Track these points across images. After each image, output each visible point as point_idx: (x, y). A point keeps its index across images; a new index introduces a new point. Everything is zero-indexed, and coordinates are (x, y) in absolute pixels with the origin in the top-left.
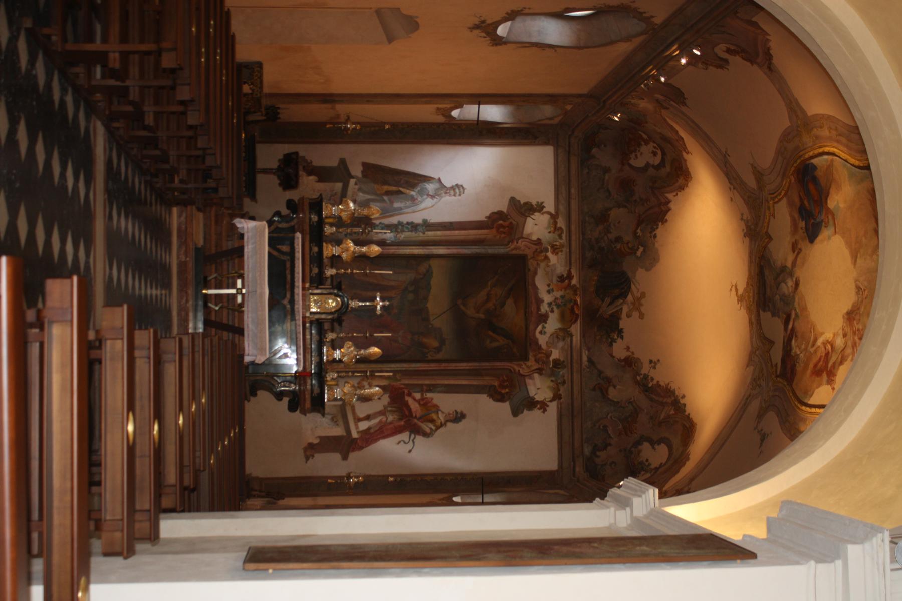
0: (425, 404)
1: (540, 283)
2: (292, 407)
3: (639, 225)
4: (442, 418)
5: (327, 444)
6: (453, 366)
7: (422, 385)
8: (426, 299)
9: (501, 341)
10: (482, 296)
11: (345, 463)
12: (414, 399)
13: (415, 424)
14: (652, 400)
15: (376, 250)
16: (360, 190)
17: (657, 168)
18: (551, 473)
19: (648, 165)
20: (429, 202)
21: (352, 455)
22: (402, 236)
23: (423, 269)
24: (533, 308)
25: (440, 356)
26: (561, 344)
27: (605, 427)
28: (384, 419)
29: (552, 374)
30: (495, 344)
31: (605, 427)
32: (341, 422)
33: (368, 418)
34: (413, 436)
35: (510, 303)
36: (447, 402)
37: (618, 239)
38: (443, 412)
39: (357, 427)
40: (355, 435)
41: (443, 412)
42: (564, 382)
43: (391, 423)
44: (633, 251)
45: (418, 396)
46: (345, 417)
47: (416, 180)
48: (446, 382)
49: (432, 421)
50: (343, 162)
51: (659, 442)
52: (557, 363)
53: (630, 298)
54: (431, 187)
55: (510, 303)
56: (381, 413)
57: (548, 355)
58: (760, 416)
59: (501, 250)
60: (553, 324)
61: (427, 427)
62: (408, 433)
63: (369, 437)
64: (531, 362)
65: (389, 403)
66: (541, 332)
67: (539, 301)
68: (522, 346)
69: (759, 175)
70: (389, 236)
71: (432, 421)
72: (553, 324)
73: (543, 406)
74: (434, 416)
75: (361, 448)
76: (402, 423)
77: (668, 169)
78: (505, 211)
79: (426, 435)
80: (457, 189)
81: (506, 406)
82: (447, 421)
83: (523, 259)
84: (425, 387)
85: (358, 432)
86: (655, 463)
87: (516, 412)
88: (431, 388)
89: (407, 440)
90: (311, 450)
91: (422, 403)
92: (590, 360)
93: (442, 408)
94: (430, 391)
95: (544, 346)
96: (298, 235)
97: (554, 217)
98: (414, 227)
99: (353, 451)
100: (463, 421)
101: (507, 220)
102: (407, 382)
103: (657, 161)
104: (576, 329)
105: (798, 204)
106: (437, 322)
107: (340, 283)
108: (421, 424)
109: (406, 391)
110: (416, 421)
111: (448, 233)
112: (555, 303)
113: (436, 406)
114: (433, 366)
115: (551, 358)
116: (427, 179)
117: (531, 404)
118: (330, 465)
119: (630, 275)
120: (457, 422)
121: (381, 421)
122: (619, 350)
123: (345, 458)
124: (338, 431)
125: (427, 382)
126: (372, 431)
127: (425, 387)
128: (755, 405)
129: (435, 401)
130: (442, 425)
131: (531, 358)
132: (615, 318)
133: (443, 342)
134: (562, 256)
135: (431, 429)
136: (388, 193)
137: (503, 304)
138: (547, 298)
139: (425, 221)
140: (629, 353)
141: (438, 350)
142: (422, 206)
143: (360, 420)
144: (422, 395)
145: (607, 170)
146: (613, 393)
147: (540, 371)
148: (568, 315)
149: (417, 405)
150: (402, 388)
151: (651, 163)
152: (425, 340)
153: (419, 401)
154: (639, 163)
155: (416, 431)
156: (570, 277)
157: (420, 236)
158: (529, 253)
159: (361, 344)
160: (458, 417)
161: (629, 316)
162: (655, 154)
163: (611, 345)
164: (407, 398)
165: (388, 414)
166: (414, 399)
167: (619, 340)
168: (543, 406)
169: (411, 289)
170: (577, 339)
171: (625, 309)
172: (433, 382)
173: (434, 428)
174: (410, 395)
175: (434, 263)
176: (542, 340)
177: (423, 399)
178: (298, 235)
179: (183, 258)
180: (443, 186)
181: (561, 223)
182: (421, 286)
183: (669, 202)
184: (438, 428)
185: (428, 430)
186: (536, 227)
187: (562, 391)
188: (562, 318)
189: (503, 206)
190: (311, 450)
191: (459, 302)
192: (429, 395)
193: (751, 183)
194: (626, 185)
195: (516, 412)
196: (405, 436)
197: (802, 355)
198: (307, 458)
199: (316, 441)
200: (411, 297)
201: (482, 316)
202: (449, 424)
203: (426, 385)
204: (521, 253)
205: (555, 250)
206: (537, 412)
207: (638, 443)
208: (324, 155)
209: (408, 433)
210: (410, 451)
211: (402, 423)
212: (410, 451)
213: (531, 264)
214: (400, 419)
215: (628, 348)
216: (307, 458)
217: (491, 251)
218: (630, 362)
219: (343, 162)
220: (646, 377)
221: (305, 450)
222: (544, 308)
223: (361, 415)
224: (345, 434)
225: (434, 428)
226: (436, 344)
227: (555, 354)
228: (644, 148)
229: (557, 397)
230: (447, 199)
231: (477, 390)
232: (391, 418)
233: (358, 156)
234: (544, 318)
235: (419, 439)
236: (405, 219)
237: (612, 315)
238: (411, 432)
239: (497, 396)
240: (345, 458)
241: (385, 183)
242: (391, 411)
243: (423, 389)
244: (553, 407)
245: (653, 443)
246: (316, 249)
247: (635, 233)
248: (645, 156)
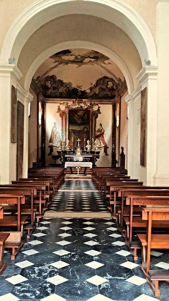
0: (98, 131)
1: (74, 107)
2: (99, 158)
3: (63, 86)
5: (105, 151)
6: (90, 126)
8: (77, 131)
9: (86, 116)
10: (76, 119)
14: (99, 85)
15: (68, 141)
16: (55, 143)
17: (51, 82)
18: (113, 106)
19: (50, 84)
20: (57, 130)
21: (108, 146)
22: (64, 135)
23: (71, 131)
24: (79, 109)
25: (89, 129)
26: (87, 103)
27: (104, 94)
29: (93, 105)
30: (86, 117)
31: (104, 94)
32: (101, 148)
33: (100, 143)
35: (78, 114)
36: (98, 127)
37: (66, 90)
42: (95, 103)
44: (68, 87)
45: (96, 133)
46: (100, 147)
47: (53, 132)
49: (102, 130)
50: (49, 147)
51: (108, 84)
52: (91, 104)
53: (78, 88)
54: (54, 129)
55: (78, 114)
56: (100, 140)
57: (89, 106)
58: (105, 64)
59: (67, 115)
60: (82, 105)
61: (103, 131)
63: (104, 143)
64: (90, 109)
66: (84, 107)
67: (78, 107)
68: (87, 111)
69: (56, 62)
70: (64, 138)
71: (102, 130)
72: (82, 105)
73: (99, 107)
75: (106, 144)
77: (51, 79)
78: (59, 114)
79: (104, 131)
80: (55, 123)
81: (99, 115)
83: (70, 111)
86: (112, 85)
87: (100, 113)
88: (95, 130)
90: (106, 154)
92: (90, 97)
95: (87, 107)
96: (65, 156)
97: (61, 104)
98: (62, 132)
101: (62, 114)
103: (49, 82)
104: (84, 100)
105: (63, 54)
106: (82, 129)
107: (74, 148)
111: (64, 126)
112: (79, 103)
114: (90, 129)
115: (90, 105)
116: (53, 129)
117: (99, 110)
118: (109, 151)
119: (73, 88)
122: (88, 91)
123: (108, 148)
124: (103, 149)
125: (94, 131)
128: (102, 64)
131: (89, 109)
132: (81, 91)
133: (86, 127)
134: (69, 102)
136: (55, 138)
137: (79, 115)
138: (77, 106)
139: (61, 130)
140: (89, 89)
141: (87, 128)
142: (58, 131)
145: (51, 92)
146: (97, 93)
147: (92, 108)
148: (81, 102)
151: (50, 83)
152: (85, 131)
154: (50, 86)
155: (103, 133)
156: (73, 101)
157: (64, 131)
158: (68, 110)
159: (87, 144)
160: (101, 125)
161: (81, 89)
162: (48, 82)
163: (87, 93)
167: (86, 91)
168: (99, 107)
169: (75, 134)
170: (86, 100)
171: (80, 90)
175: (70, 129)
176: (86, 107)
178: (65, 156)
179: (73, 178)
180: (54, 126)
181: (62, 102)
182: (74, 132)
183: (58, 80)
186: (63, 108)
187: (96, 103)
188: (81, 103)
189: (58, 114)
190: (106, 154)
191: (78, 124)
192: (96, 131)
193: (57, 63)
194: (54, 88)
195: (100, 113)
197: (94, 55)
198: (108, 155)
199: (105, 153)
200: (77, 134)
201: (81, 119)
204: (68, 111)
205: (67, 104)
206: (100, 109)
207: (107, 87)
208: (48, 150)
213: (70, 109)
215: (88, 89)
216: (108, 155)
217: (68, 117)
218: (91, 89)
219: (49, 147)
220: (94, 86)
221: (106, 155)
222: (79, 106)
226: (86, 129)
227: (89, 104)
228: (47, 85)
229: (97, 104)
230: (57, 126)
231: (95, 121)
233: (48, 144)
234: (81, 107)
236: (61, 135)
237: (81, 92)
238: (103, 134)
239: (97, 117)
240: (108, 148)
241: (53, 138)
243: (95, 132)
244: (99, 105)
245: (108, 85)
246: (68, 153)
247: (65, 87)
248: (49, 84)
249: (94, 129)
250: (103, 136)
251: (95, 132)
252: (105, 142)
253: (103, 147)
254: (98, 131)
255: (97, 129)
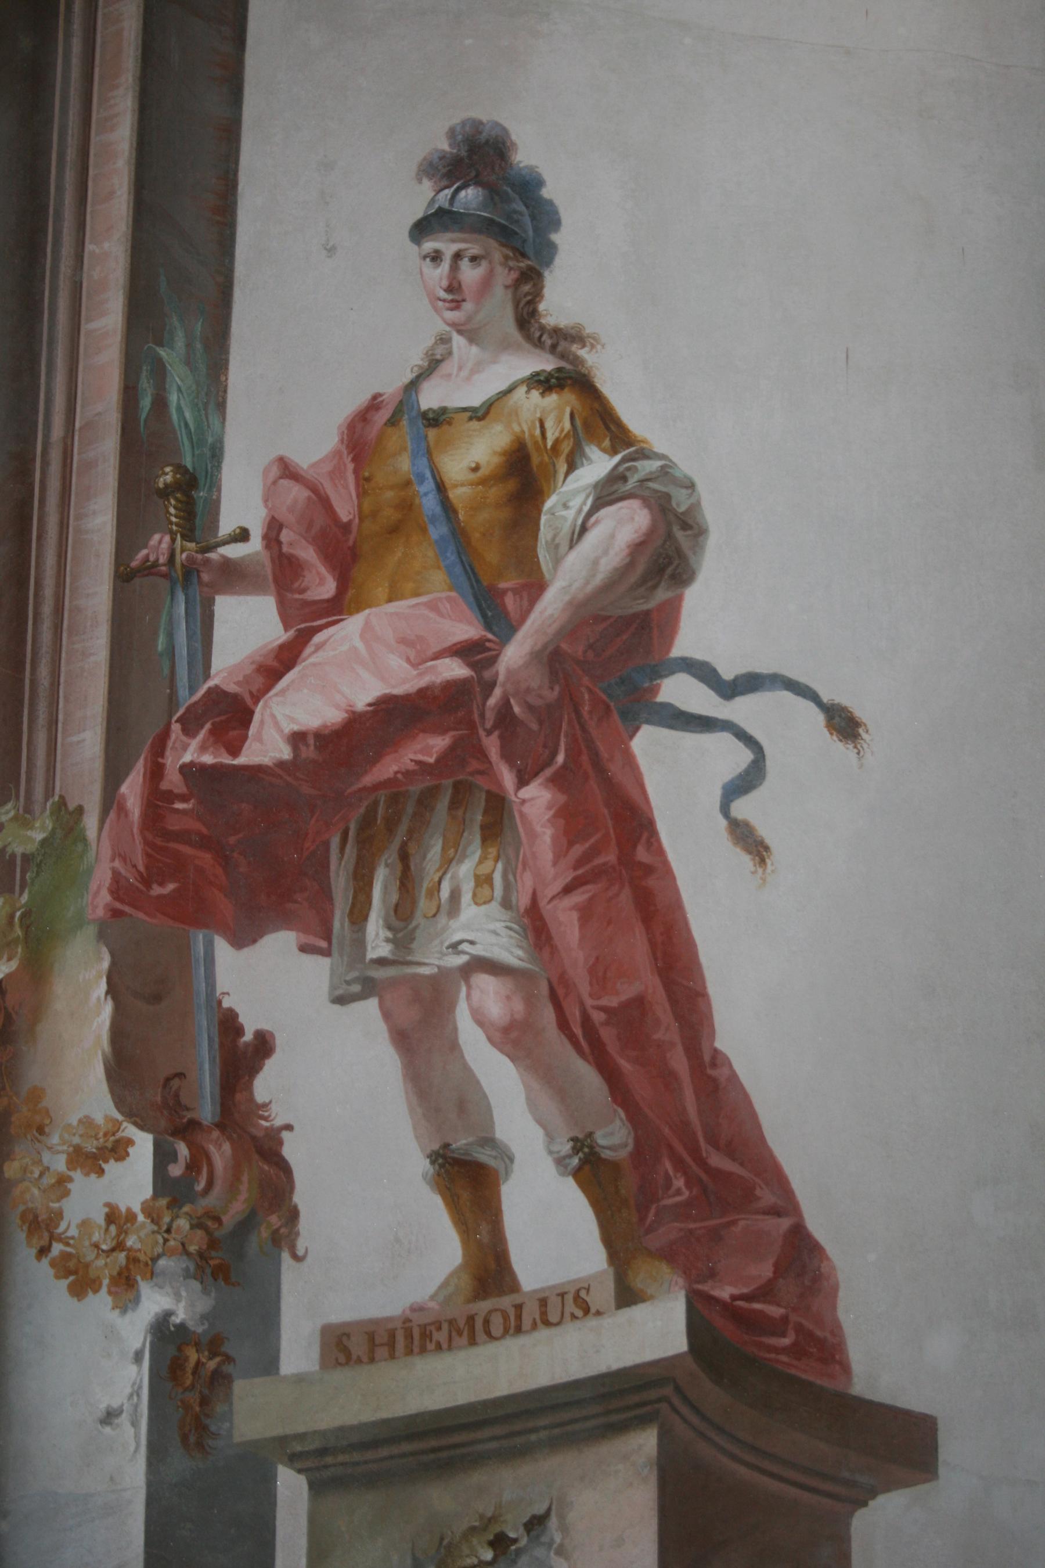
0: (336, 554)
4: (491, 374)
7: (125, 576)
11: (952, 1449)
12: (280, 663)
13: (552, 659)
28: (490, 996)
32: (510, 1488)
33: (468, 1180)
34: (679, 691)
36: (328, 322)
38: (432, 365)
39: (574, 1303)
40: (657, 1329)
41: (432, 365)
43: (536, 926)
45: (245, 626)
46: (448, 1442)
48: (108, 319)
49: (524, 477)
56: (420, 1027)
61: (585, 543)
62: (648, 744)
65: (319, 940)
71: (524, 477)
74: (475, 453)
75: (800, 1254)
76: (536, 801)
79: (667, 556)
82: (526, 317)
84: (158, 545)
85: (627, 1296)
88: (169, 482)
89: (727, 757)
91: (325, 588)
93: (390, 383)
94: (192, 497)
99: (826, 1349)
100: (527, 154)
102: (86, 743)
108: (551, 607)
109: (192, 751)
110: (514, 653)
113: (363, 438)
120: (546, 217)
121: (512, 1038)
123: (905, 1445)
125: (99, 518)
126: (614, 1137)
127: (158, 545)
129: (315, 444)
130: (572, 380)
135: (606, 494)
143: (489, 1268)
144: (234, 577)
149: (348, 633)
150: (157, 800)
153: (306, 621)
160: (491, 206)
164: (266, 745)
165: (433, 959)
166: (280, 663)
172: (106, 449)
173: (598, 465)
174: (230, 715)
177: (284, 574)
184: (600, 421)
185: (624, 525)
192: (242, 502)
196: (675, 774)
202: (561, 301)
203: (129, 530)
209: (648, 744)
210: (844, 724)
211: (536, 801)
212: (844, 724)
214: (497, 822)
223: (445, 1251)
224: (646, 1442)
225: (598, 465)
232: (481, 927)
235: (710, 622)
238: (639, 706)
242: (402, 915)
249: (143, 441)
250: (617, 843)
251: (203, 578)
252: (713, 1079)
253: (612, 1402)
254: (336, 554)
255: (277, 420)
